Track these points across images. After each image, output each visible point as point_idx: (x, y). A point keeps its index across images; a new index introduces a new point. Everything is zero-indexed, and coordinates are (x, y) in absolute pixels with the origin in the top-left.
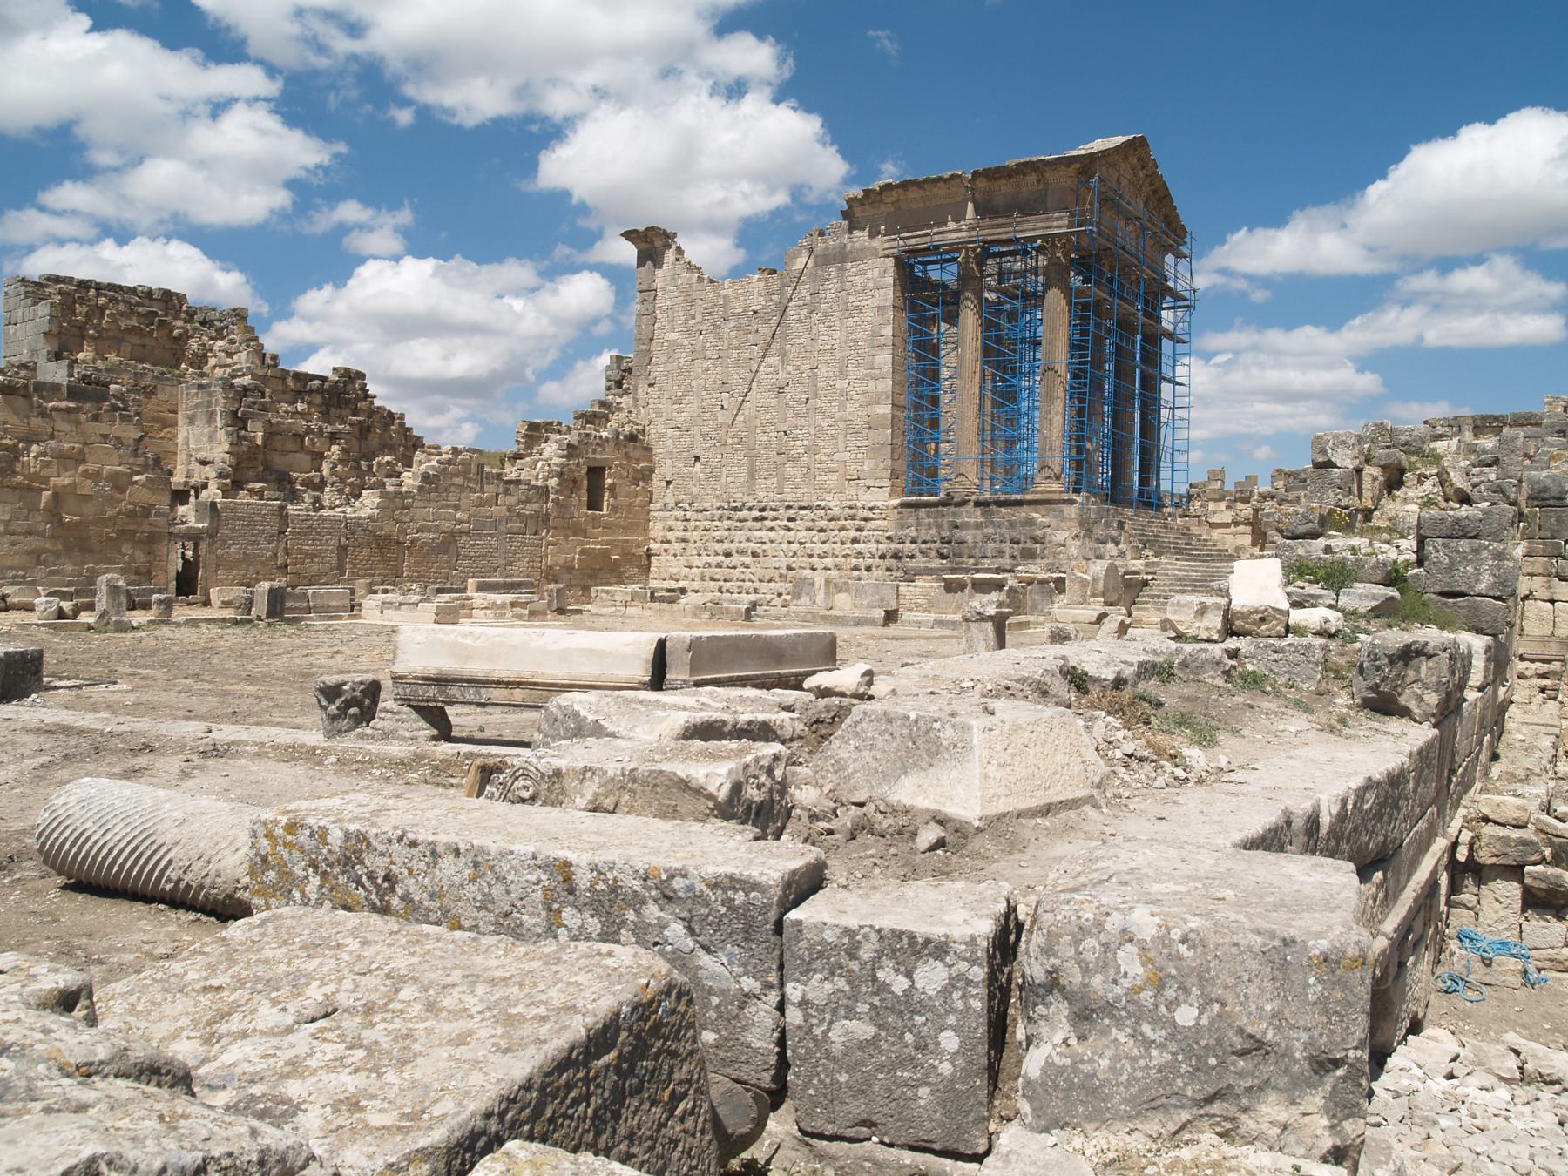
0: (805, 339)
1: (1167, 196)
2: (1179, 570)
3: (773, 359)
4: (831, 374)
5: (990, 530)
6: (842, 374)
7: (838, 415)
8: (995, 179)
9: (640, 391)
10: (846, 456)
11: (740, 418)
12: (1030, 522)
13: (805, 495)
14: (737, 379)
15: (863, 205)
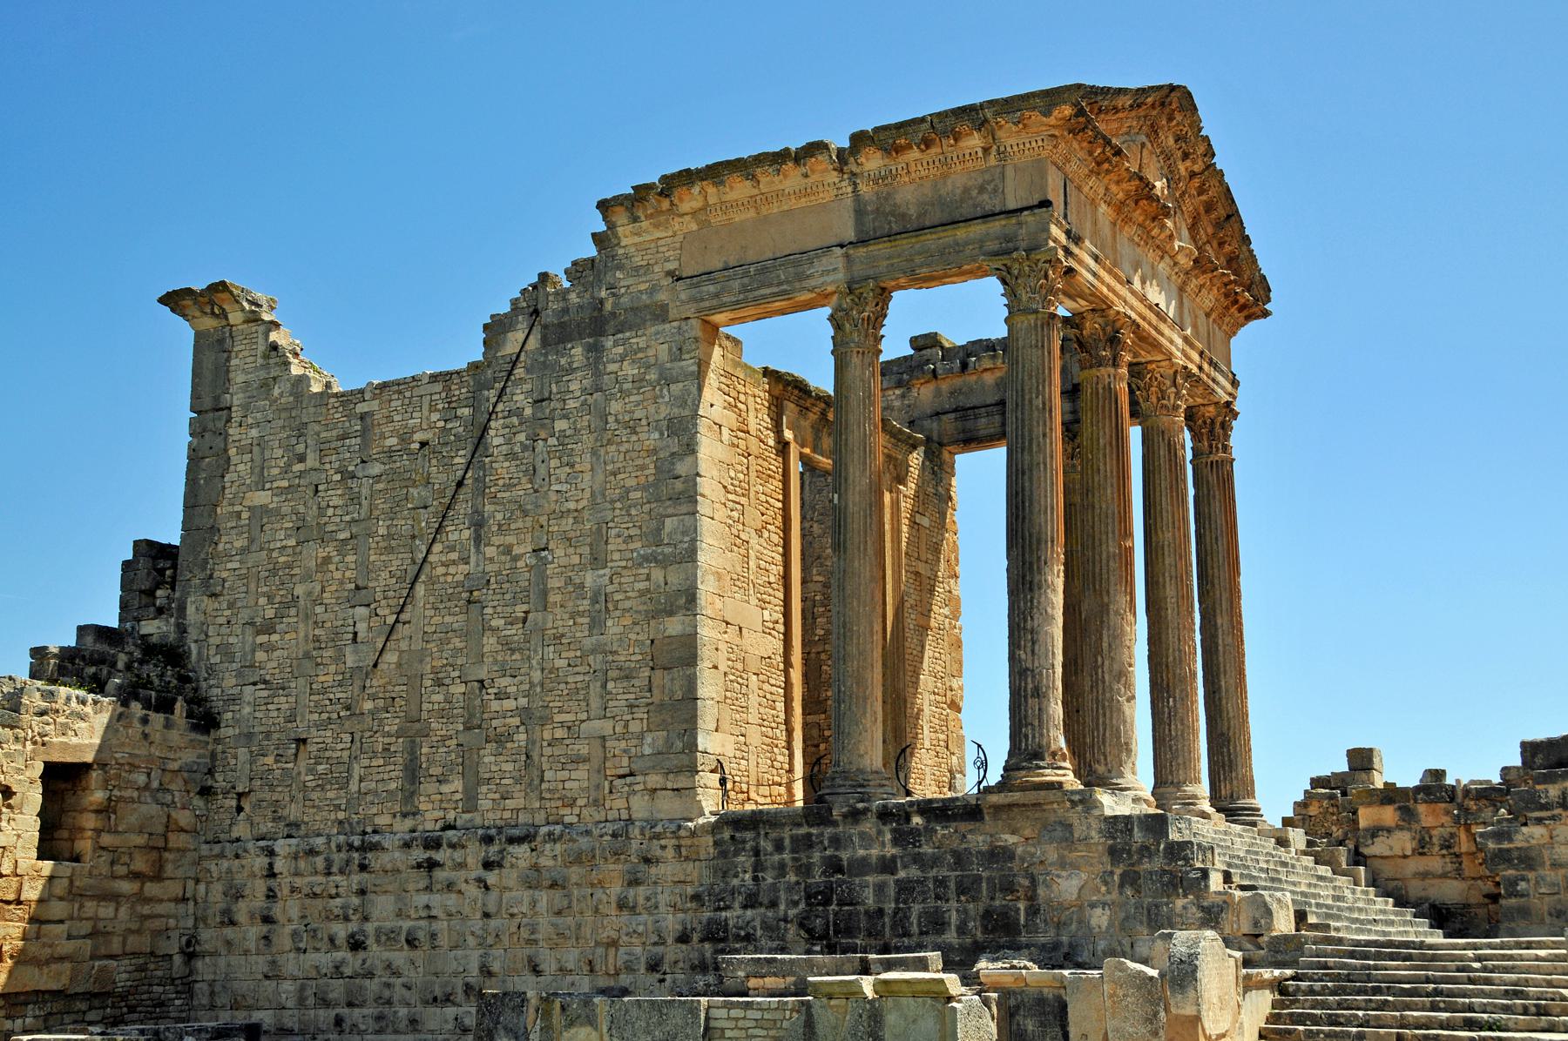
0: (523, 489)
1: (1233, 215)
2: (1352, 955)
3: (458, 533)
4: (576, 559)
5: (914, 872)
6: (597, 561)
7: (588, 643)
8: (899, 150)
9: (191, 609)
10: (606, 727)
11: (391, 657)
12: (998, 855)
13: (519, 806)
14: (381, 582)
15: (635, 220)
